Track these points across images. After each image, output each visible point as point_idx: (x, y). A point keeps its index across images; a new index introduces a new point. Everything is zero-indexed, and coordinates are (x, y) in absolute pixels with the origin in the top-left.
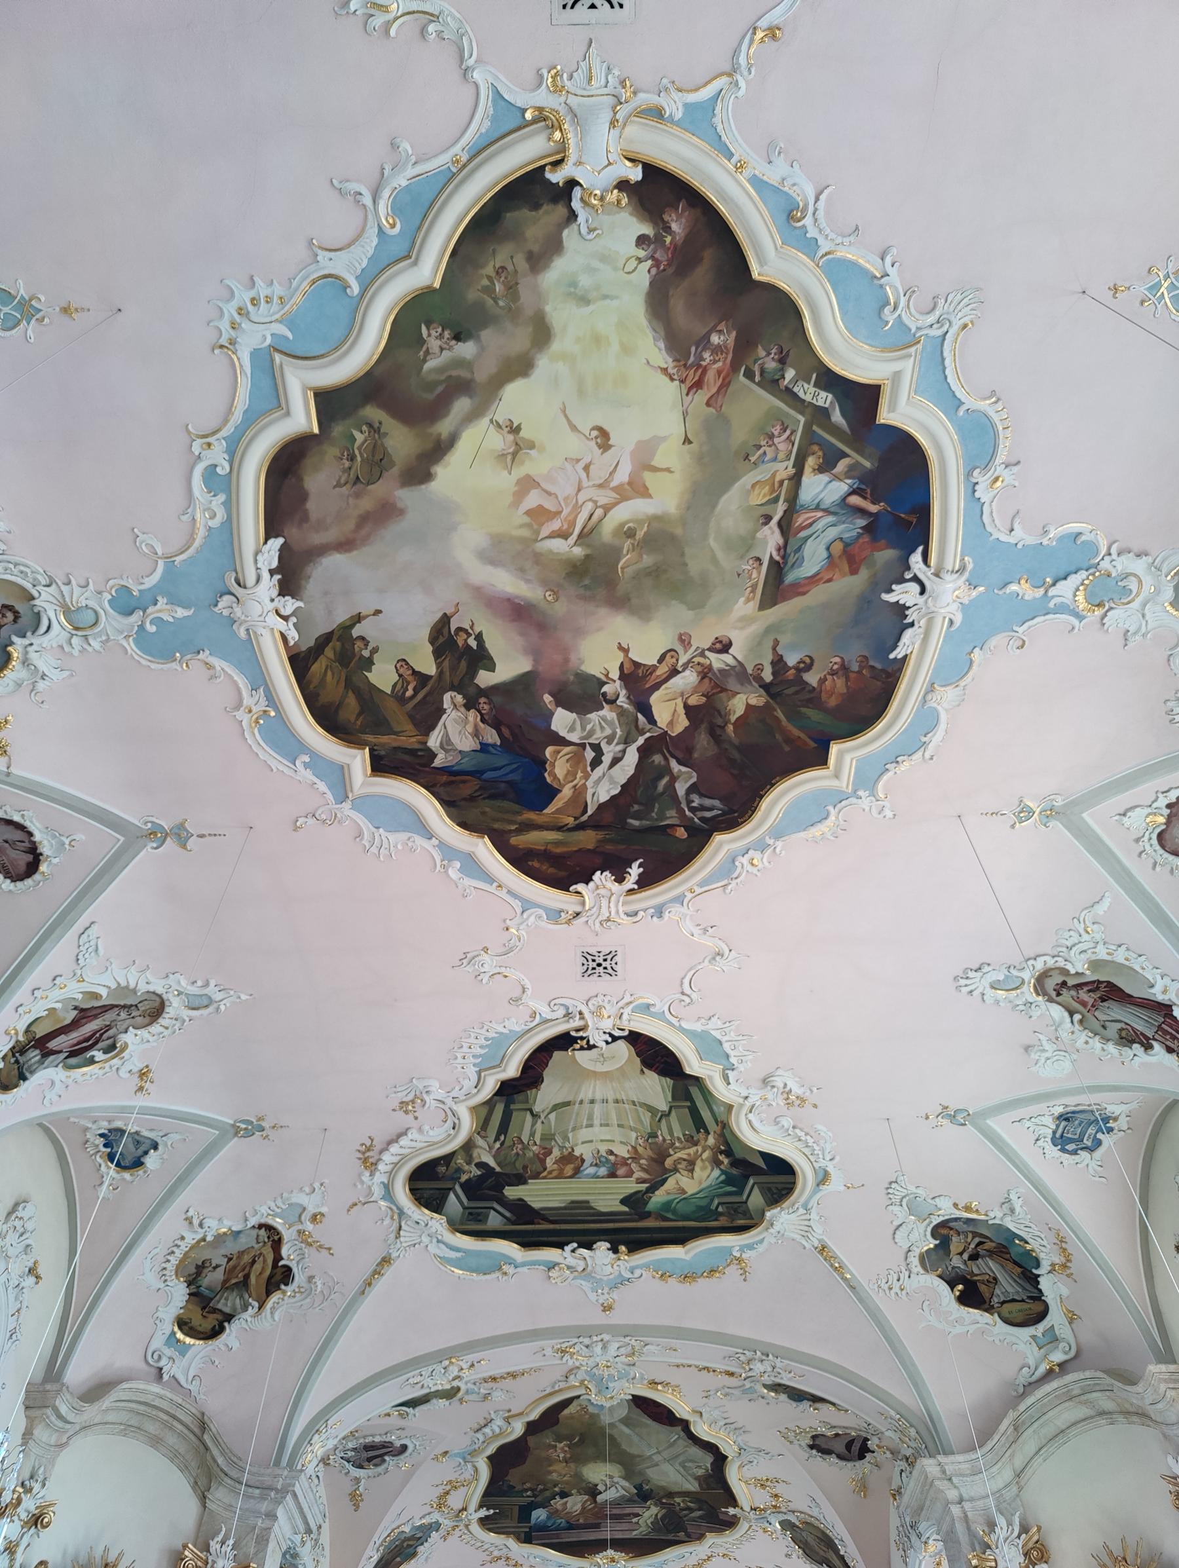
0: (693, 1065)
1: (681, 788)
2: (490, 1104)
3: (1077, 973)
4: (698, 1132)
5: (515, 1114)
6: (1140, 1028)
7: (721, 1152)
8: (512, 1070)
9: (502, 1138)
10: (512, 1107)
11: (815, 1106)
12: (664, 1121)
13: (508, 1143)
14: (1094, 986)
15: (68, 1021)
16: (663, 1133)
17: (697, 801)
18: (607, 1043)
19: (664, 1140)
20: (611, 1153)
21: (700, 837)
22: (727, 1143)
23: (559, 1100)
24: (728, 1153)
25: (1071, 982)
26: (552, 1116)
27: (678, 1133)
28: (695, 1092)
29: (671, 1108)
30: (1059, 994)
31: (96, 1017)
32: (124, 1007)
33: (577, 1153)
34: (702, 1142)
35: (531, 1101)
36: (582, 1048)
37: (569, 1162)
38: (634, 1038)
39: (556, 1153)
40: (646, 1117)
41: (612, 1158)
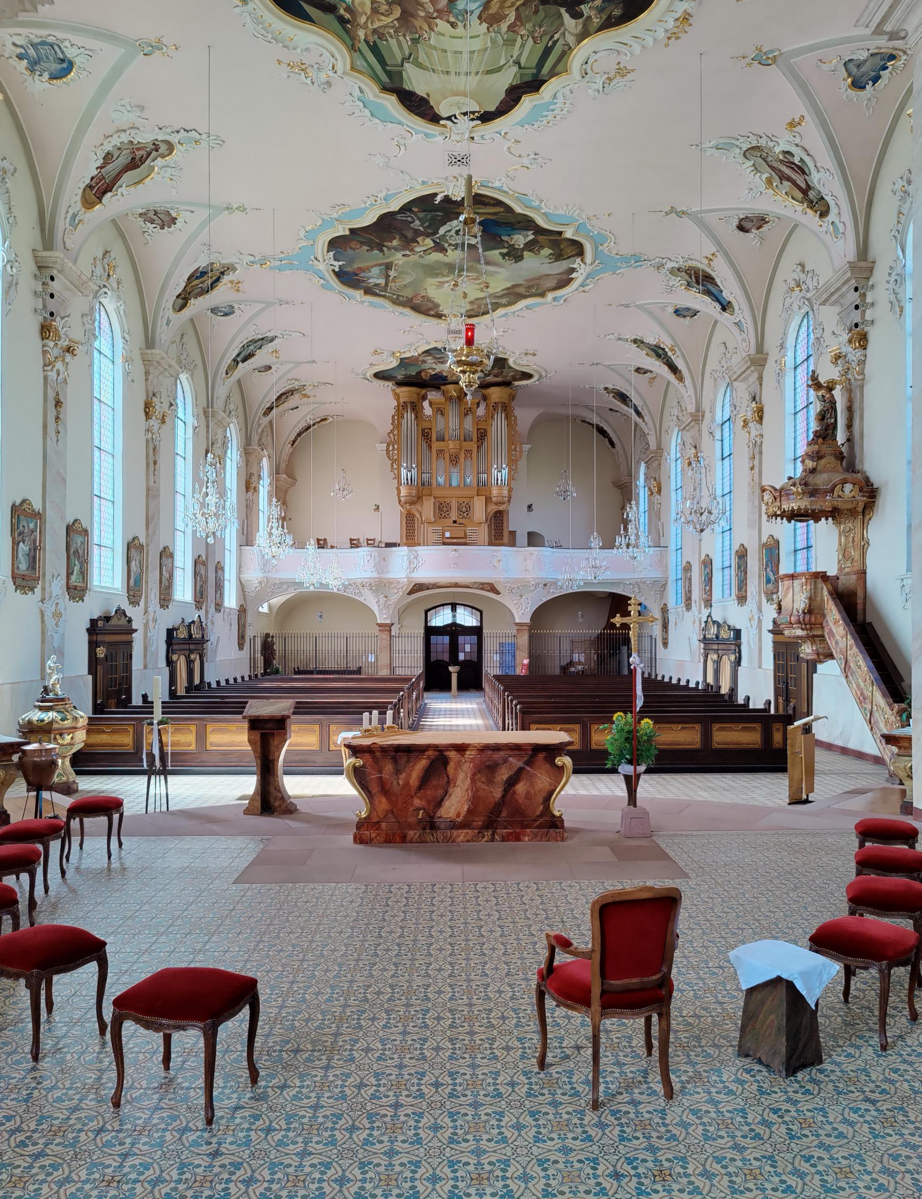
0: (391, 102)
1: (417, 222)
2: (553, 74)
3: (156, 159)
4: (374, 42)
5: (534, 65)
6: (108, 167)
7: (348, 21)
8: (527, 102)
9: (550, 43)
10: (535, 71)
11: (279, 62)
12: (407, 54)
13: (548, 37)
14: (142, 160)
15: (789, 183)
16: (406, 42)
17: (409, 219)
18: (455, 116)
19: (404, 36)
20: (453, 25)
21: (406, 208)
22: (347, 31)
23: (495, 76)
24: (342, 21)
25: (154, 153)
26: (503, 62)
27: (393, 42)
28: (385, 79)
29: (402, 66)
30: (154, 144)
31: (780, 171)
32: (766, 161)
33: (485, 25)
34: (369, 33)
35: (518, 75)
36: (473, 113)
37: (493, 15)
38: (435, 119)
39: (504, 26)
40: (422, 58)
41: (452, 19)
